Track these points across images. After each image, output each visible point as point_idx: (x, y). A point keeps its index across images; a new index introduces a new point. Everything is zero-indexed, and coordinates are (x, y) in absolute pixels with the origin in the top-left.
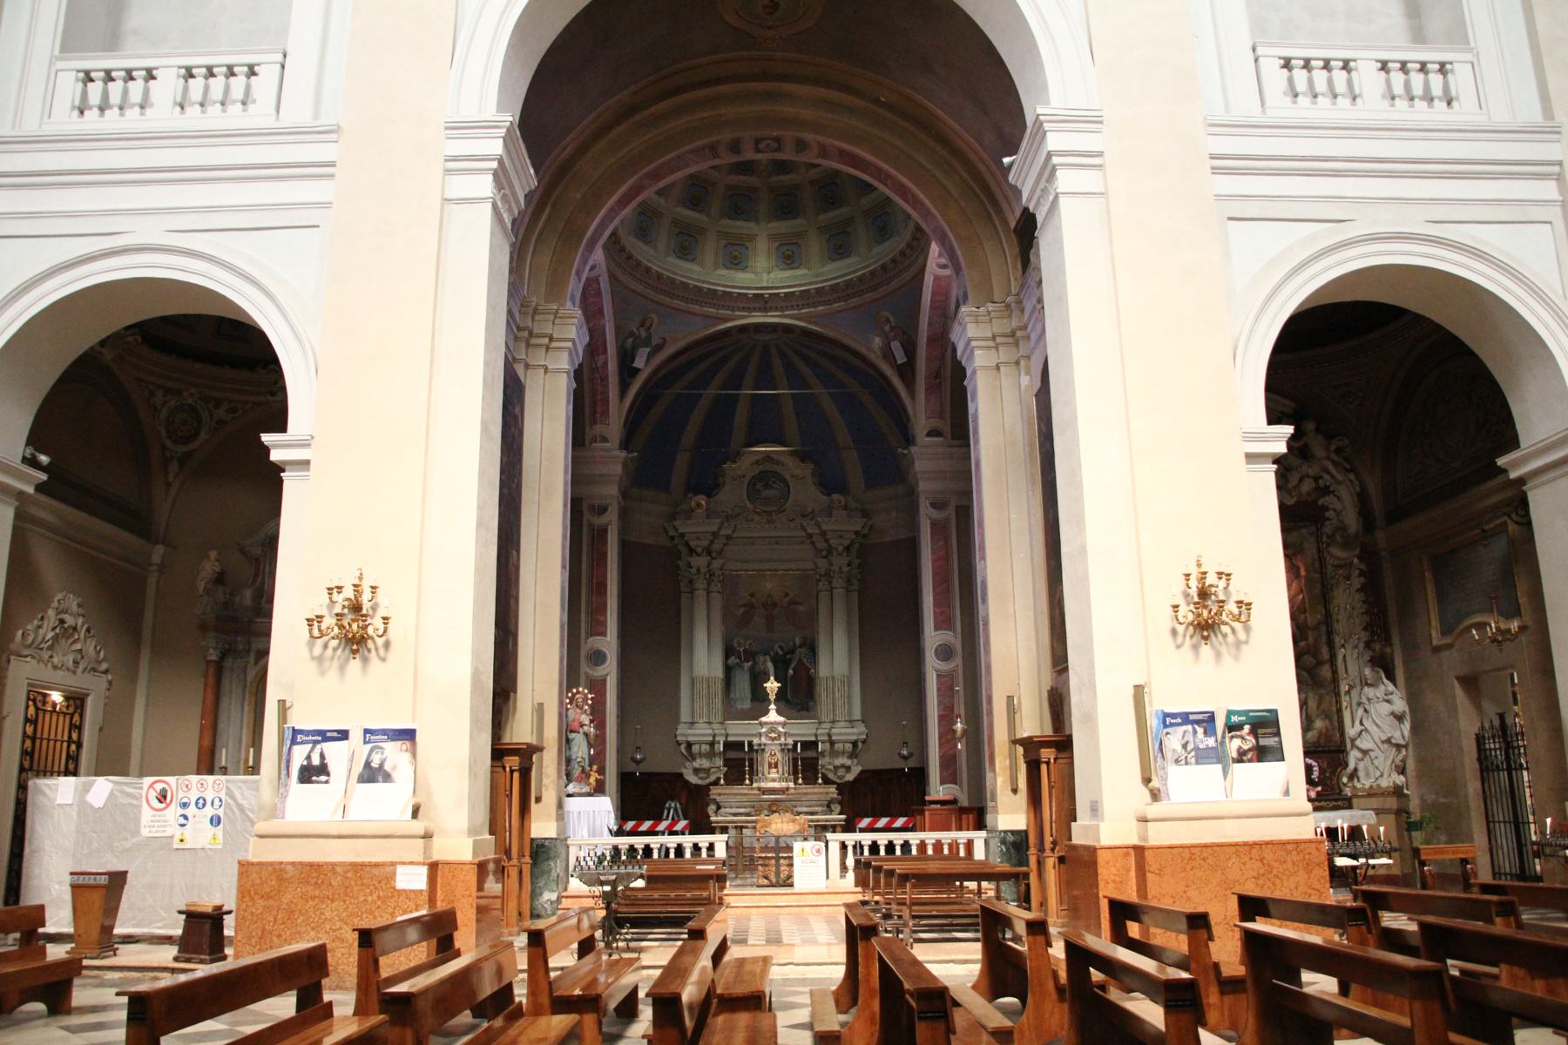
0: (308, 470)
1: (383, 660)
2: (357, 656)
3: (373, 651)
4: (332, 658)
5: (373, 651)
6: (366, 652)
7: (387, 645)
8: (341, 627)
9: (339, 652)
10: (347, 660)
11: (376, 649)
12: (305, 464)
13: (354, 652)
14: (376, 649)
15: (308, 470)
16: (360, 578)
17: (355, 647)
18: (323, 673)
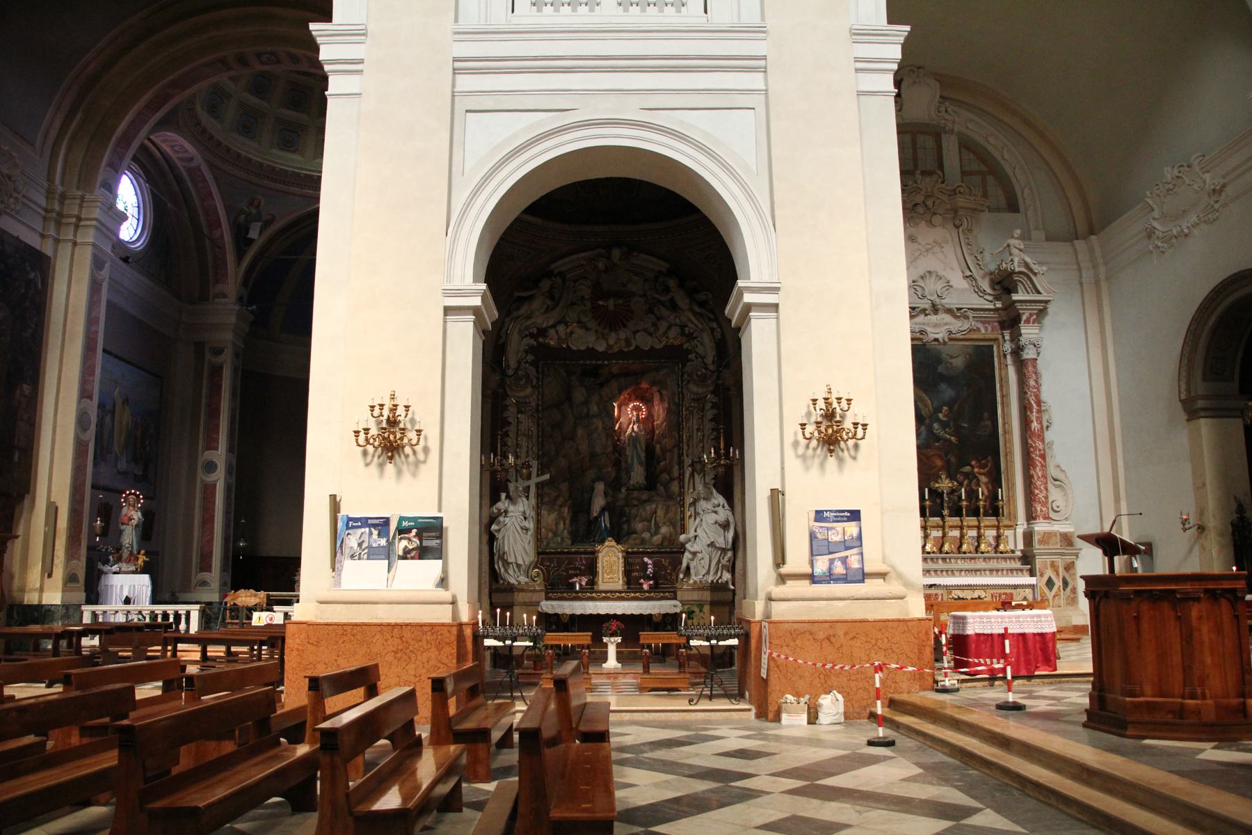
1: (854, 458)
3: (846, 452)
4: (814, 456)
5: (846, 452)
6: (840, 453)
8: (820, 432)
9: (819, 451)
10: (826, 457)
11: (848, 449)
13: (831, 451)
14: (848, 449)
16: (830, 393)
17: (832, 448)
18: (807, 468)
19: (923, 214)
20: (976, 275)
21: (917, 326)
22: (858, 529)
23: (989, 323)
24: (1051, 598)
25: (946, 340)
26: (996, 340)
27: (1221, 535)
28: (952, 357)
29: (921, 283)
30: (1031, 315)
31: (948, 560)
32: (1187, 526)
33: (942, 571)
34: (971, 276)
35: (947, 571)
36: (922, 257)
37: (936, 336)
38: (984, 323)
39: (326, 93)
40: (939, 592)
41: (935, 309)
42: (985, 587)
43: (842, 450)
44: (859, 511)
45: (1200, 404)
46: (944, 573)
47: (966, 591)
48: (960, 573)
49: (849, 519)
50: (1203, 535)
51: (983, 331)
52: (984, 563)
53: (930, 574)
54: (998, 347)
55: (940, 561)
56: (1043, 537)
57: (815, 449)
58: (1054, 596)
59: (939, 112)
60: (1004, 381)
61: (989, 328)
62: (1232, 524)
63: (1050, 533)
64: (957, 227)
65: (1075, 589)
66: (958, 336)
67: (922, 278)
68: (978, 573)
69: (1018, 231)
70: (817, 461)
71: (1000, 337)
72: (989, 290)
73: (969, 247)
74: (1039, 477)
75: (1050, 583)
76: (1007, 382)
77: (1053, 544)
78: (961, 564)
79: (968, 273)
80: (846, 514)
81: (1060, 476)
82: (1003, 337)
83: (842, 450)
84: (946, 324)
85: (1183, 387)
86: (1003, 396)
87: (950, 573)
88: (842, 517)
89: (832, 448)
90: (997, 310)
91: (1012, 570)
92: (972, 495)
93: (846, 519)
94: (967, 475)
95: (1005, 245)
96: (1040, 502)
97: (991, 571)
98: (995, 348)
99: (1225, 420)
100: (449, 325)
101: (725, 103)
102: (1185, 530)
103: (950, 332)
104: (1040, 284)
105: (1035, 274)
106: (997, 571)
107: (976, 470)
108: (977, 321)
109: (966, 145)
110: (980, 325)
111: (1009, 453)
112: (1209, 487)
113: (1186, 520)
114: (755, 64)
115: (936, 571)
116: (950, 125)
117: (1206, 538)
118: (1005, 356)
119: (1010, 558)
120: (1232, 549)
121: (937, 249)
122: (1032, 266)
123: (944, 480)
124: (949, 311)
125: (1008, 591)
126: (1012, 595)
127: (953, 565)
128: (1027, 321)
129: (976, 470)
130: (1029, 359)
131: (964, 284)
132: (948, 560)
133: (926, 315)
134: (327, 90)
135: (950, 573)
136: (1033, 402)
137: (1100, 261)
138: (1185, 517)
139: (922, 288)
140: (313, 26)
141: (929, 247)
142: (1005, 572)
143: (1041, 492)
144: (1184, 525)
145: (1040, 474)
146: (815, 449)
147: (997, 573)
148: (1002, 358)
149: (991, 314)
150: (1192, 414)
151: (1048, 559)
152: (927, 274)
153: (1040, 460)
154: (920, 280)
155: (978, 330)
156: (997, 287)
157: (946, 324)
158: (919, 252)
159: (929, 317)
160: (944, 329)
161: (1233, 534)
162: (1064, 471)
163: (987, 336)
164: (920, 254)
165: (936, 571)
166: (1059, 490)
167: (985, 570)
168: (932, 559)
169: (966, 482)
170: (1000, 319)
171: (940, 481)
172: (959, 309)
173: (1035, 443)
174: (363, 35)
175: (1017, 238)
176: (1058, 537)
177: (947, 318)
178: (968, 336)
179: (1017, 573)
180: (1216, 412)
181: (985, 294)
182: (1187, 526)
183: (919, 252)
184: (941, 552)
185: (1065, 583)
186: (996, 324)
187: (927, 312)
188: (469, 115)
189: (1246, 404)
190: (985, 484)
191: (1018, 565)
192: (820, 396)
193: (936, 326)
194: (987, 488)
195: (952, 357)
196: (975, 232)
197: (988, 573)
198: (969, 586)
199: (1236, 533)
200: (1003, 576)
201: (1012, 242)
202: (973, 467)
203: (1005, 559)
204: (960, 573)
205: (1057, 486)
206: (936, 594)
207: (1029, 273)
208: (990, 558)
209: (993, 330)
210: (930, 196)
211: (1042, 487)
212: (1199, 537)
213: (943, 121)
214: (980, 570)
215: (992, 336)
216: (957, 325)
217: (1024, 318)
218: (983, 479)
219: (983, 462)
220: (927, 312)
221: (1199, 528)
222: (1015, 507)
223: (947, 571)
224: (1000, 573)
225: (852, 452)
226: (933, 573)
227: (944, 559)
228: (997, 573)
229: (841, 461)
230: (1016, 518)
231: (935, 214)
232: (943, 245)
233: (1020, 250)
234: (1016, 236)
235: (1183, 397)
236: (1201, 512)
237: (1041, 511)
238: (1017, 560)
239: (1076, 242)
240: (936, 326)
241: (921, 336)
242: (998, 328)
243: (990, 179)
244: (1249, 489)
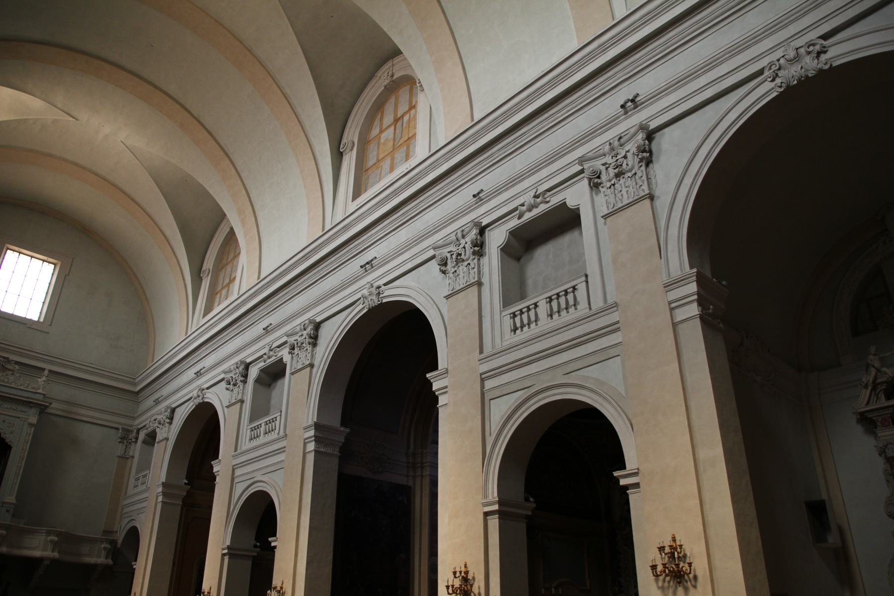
0: (639, 487)
2: (681, 585)
3: (689, 583)
5: (689, 583)
6: (685, 583)
7: (695, 577)
9: (672, 583)
10: (676, 588)
11: (690, 580)
12: (637, 485)
14: (690, 580)
15: (639, 487)
39: (438, 406)
43: (687, 582)
57: (669, 582)
70: (671, 591)
89: (678, 580)
100: (489, 522)
101: (603, 357)
114: (613, 328)
134: (438, 404)
140: (428, 375)
146: (669, 582)
174: (446, 373)
188: (491, 401)
192: (667, 542)
225: (693, 582)
229: (686, 589)
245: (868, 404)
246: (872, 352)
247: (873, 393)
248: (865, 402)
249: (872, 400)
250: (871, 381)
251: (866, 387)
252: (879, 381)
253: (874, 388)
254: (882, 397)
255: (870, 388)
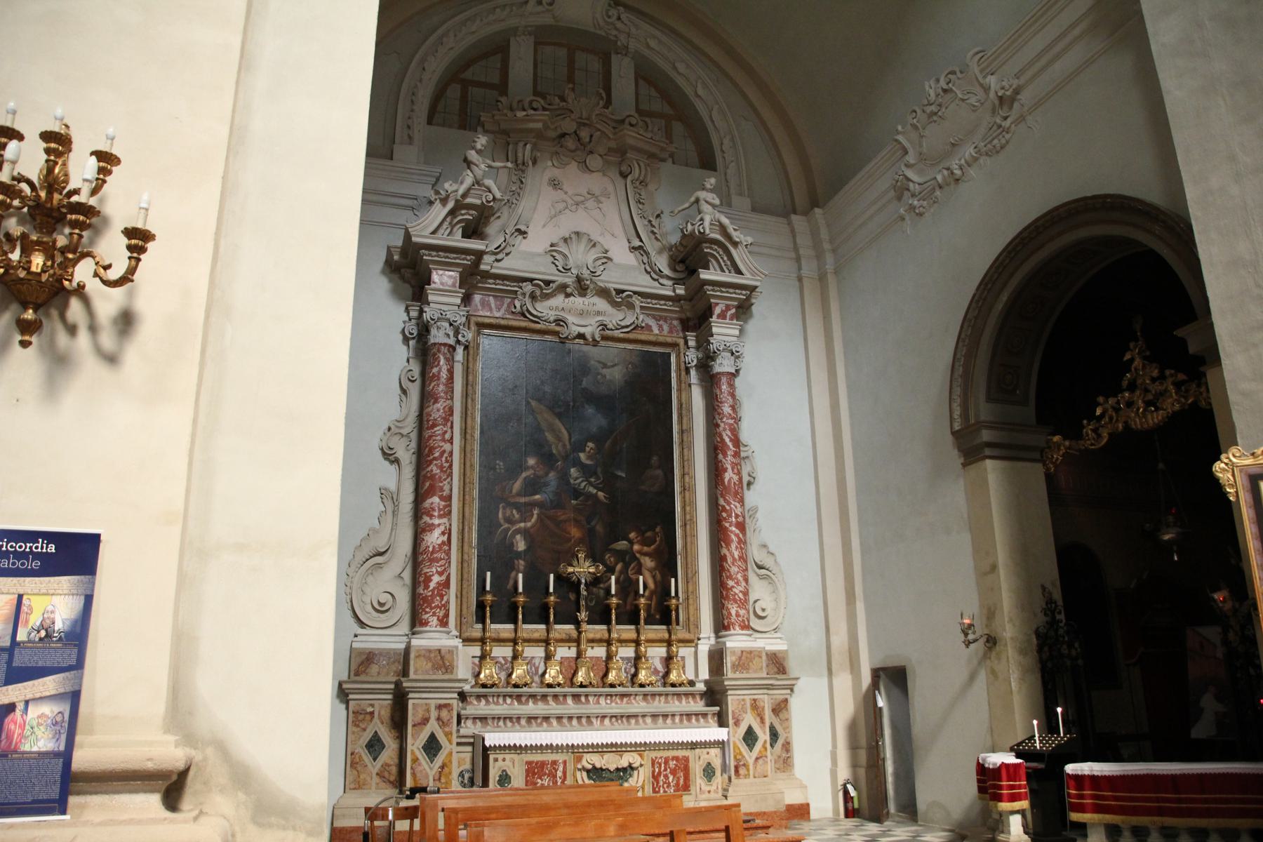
1: (111, 359)
2: (34, 339)
3: (83, 338)
5: (83, 338)
6: (62, 338)
7: (126, 321)
11: (93, 329)
13: (27, 328)
14: (93, 329)
17: (29, 315)
19: (572, 151)
20: (649, 248)
21: (553, 313)
22: (78, 603)
23: (665, 320)
24: (751, 761)
25: (598, 338)
26: (674, 345)
27: (1022, 652)
28: (605, 366)
29: (563, 248)
30: (728, 308)
31: (583, 699)
32: (971, 637)
33: (570, 718)
34: (640, 247)
35: (579, 718)
36: (567, 211)
37: (582, 330)
38: (654, 317)
40: (560, 757)
41: (582, 287)
42: (639, 748)
43: (72, 330)
44: (94, 540)
45: (986, 435)
46: (575, 722)
47: (606, 756)
48: (602, 722)
49: (49, 567)
50: (994, 654)
51: (656, 331)
52: (643, 704)
53: (550, 724)
54: (678, 356)
55: (569, 700)
56: (740, 658)
58: (757, 759)
59: (609, 17)
60: (686, 409)
61: (666, 328)
62: (1037, 633)
63: (751, 652)
64: (624, 176)
65: (788, 743)
66: (617, 333)
67: (565, 240)
68: (633, 721)
69: (713, 181)
71: (681, 342)
72: (667, 271)
73: (641, 206)
74: (734, 559)
75: (750, 738)
76: (690, 410)
77: (755, 672)
78: (606, 706)
79: (637, 243)
80: (40, 547)
81: (767, 561)
82: (686, 342)
83: (72, 330)
84: (598, 313)
85: (957, 412)
86: (682, 432)
87: (584, 720)
88: (24, 555)
89: (29, 315)
90: (676, 299)
91: (689, 715)
92: (628, 587)
93: (36, 564)
94: (623, 556)
95: (693, 199)
96: (735, 601)
97: (654, 716)
98: (673, 359)
99: (1020, 464)
102: (968, 644)
103: (604, 326)
104: (743, 260)
105: (735, 244)
106: (665, 716)
107: (636, 547)
108: (648, 315)
109: (647, 75)
110: (652, 322)
111: (689, 523)
112: (1002, 572)
113: (970, 626)
115: (559, 718)
116: (623, 39)
117: (999, 659)
118: (687, 370)
119: (687, 695)
120: (1039, 676)
121: (591, 203)
122: (730, 229)
123: (581, 561)
124: (604, 293)
125: (681, 753)
126: (686, 759)
127: (592, 707)
128: (722, 316)
129: (636, 547)
130: (722, 374)
131: (631, 259)
132: (583, 699)
133: (568, 295)
135: (584, 720)
136: (727, 440)
137: (827, 246)
138: (967, 621)
139: (565, 256)
141: (580, 199)
142: (677, 719)
143: (737, 583)
144: (966, 635)
145: (736, 554)
147: (665, 721)
148: (683, 373)
149: (668, 306)
150: (971, 452)
151: (748, 696)
152: (573, 236)
153: (737, 531)
154: (561, 243)
155: (649, 328)
156: (680, 267)
157: (598, 313)
158: (562, 206)
159: (572, 298)
160: (593, 321)
161: (1040, 649)
162: (772, 554)
163: (661, 339)
164: (567, 208)
165: (559, 718)
166: (764, 583)
167: (644, 716)
168: (555, 696)
169: (619, 567)
170: (683, 316)
171: (575, 563)
172: (620, 292)
173: (729, 504)
175: (711, 191)
176: (764, 658)
177: (601, 304)
178: (631, 336)
179: (697, 720)
180: (1009, 452)
181: (662, 277)
182: (971, 637)
183: (562, 206)
184: (572, 685)
185: (774, 735)
186: (675, 323)
187: (569, 290)
189: (1048, 441)
190: (651, 571)
191: (698, 706)
193: (581, 314)
194: (654, 577)
195: (605, 366)
196: (651, 187)
197: (649, 720)
198: (612, 745)
199: (1046, 649)
200: (674, 726)
201: (702, 195)
202: (631, 542)
203: (678, 695)
204: (602, 722)
205: (761, 577)
206: (554, 763)
207: (726, 244)
208: (654, 695)
209: (671, 331)
210: (585, 125)
211: (739, 576)
212: (985, 656)
213: (615, 32)
214: (635, 716)
215: (669, 340)
216: (615, 317)
217: (717, 310)
218: (648, 562)
219: (649, 534)
220: (569, 290)
221: (988, 641)
222: (698, 609)
223: (579, 718)
224: (669, 721)
225: (107, 340)
226: (554, 722)
227: (576, 697)
228: (665, 721)
230: (697, 626)
231: (591, 152)
232: (602, 199)
233: (713, 206)
234: (708, 186)
235: (957, 427)
236: (990, 614)
237: (738, 615)
238: (698, 698)
239: (794, 217)
240: (581, 314)
241: (558, 329)
242: (679, 328)
243: (678, 128)
244: (1058, 577)
245: (433, 233)
246: (479, 146)
247: (448, 219)
248: (432, 229)
249: (441, 231)
250: (461, 192)
251: (444, 201)
252: (469, 200)
253: (452, 213)
254: (458, 233)
255: (451, 205)
